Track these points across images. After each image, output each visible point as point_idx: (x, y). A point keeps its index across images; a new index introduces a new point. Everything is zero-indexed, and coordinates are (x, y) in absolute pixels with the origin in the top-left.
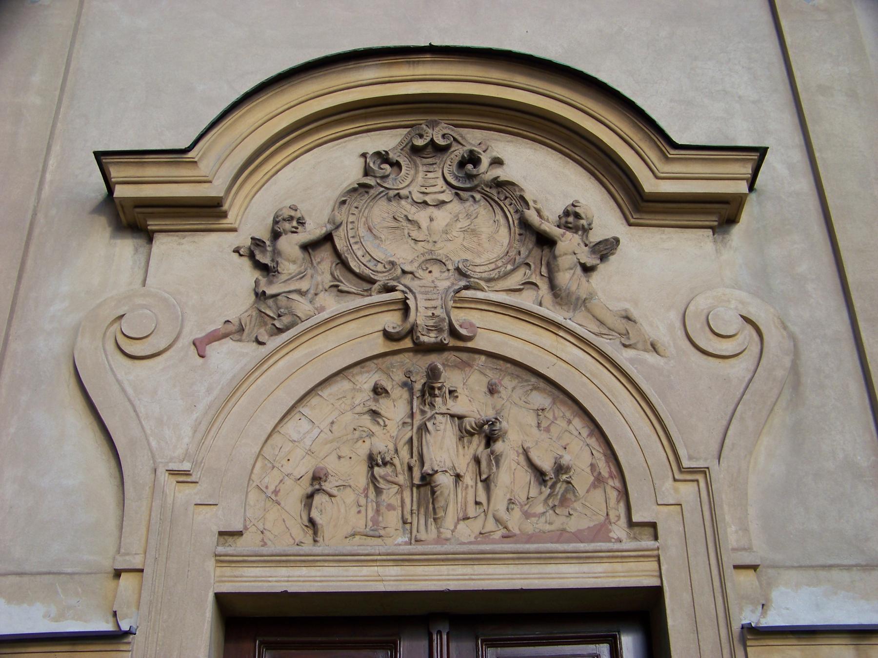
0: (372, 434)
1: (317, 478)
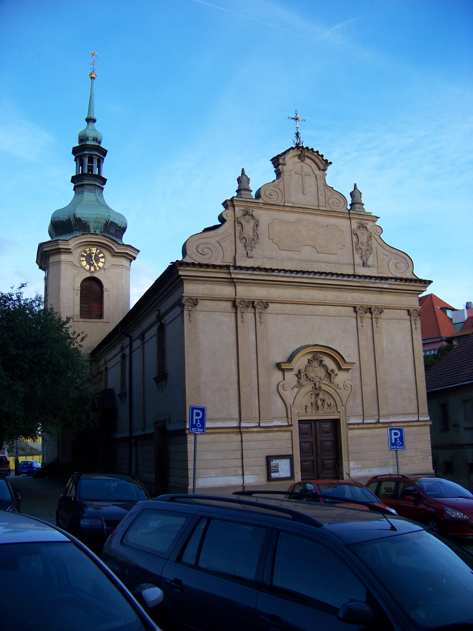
0: (311, 400)
1: (306, 406)
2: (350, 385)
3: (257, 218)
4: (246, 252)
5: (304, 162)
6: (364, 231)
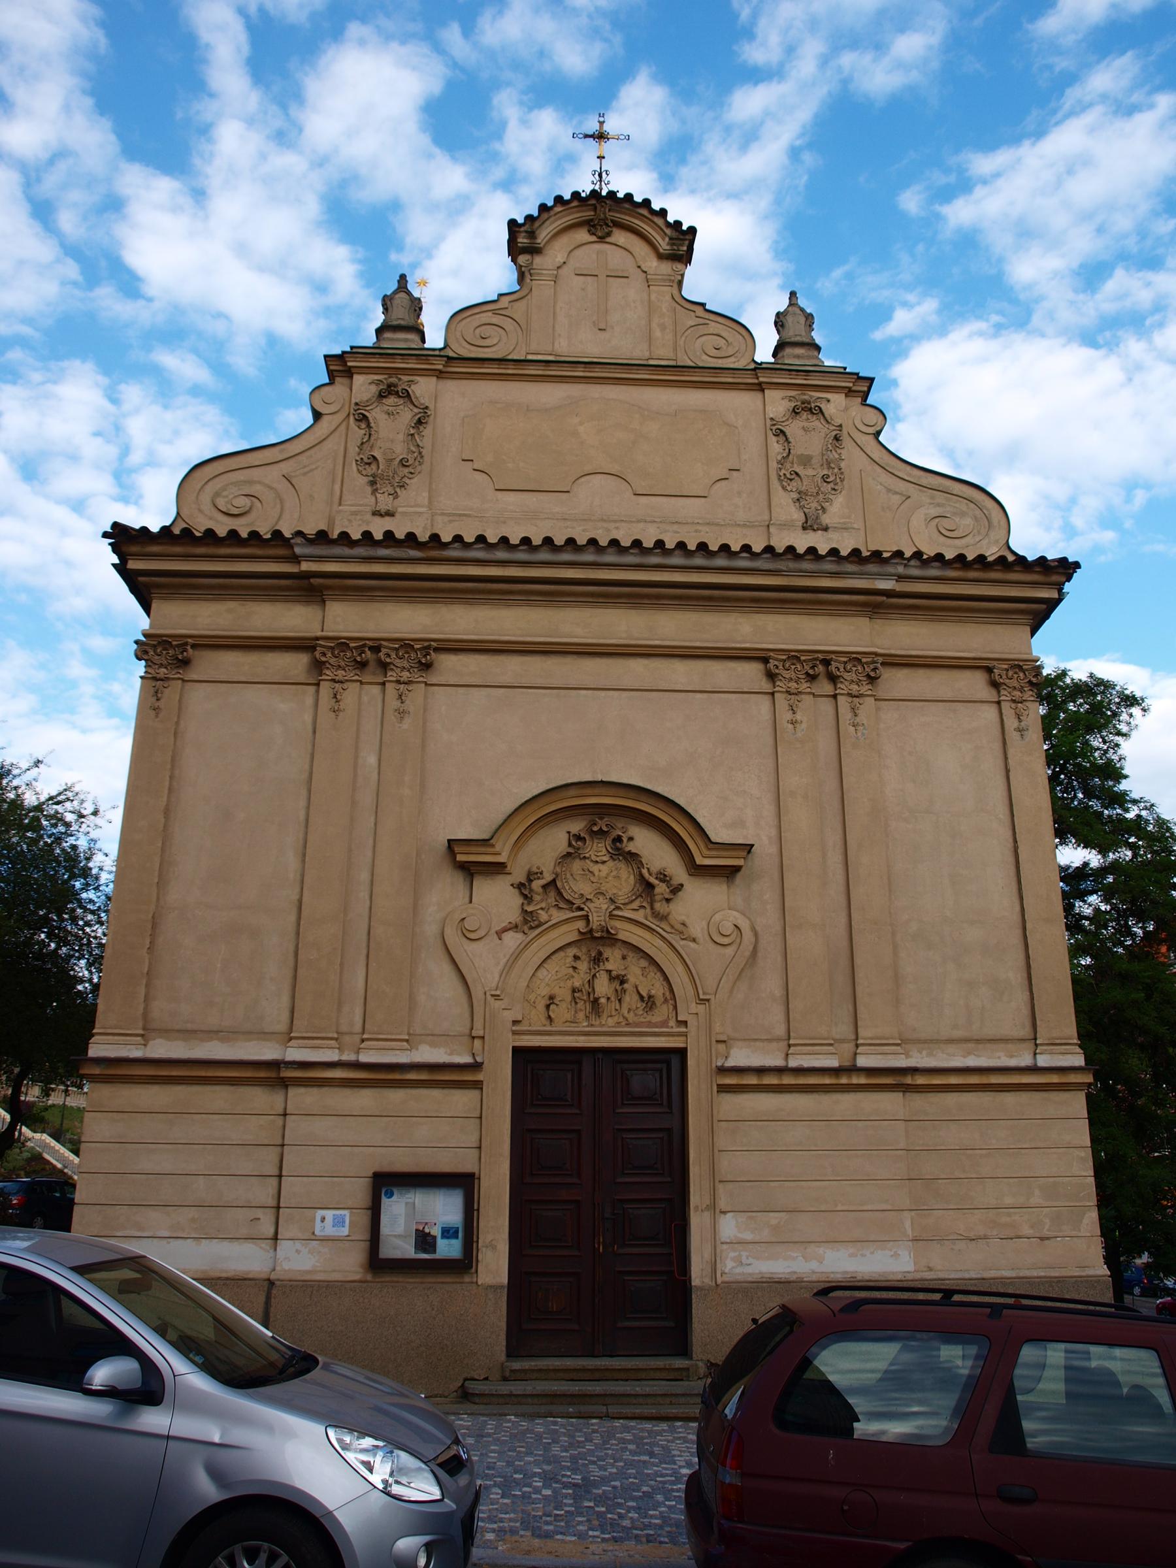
0: (573, 977)
1: (552, 998)
3: (423, 401)
6: (816, 423)
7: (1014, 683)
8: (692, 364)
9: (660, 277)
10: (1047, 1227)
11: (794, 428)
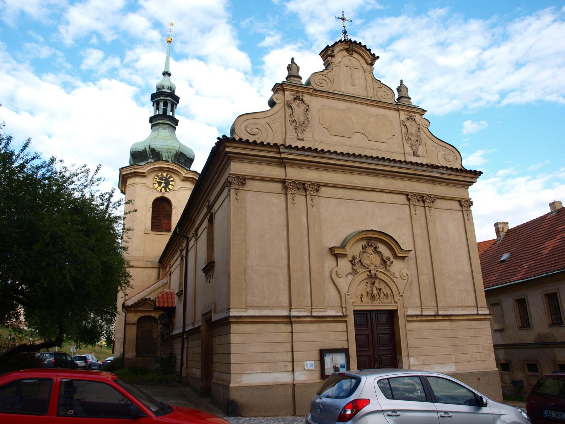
0: (366, 289)
1: (362, 295)
2: (407, 274)
3: (307, 103)
4: (296, 134)
5: (352, 56)
6: (413, 123)
7: (465, 205)
8: (379, 100)
9: (368, 70)
10: (484, 358)
11: (408, 124)
